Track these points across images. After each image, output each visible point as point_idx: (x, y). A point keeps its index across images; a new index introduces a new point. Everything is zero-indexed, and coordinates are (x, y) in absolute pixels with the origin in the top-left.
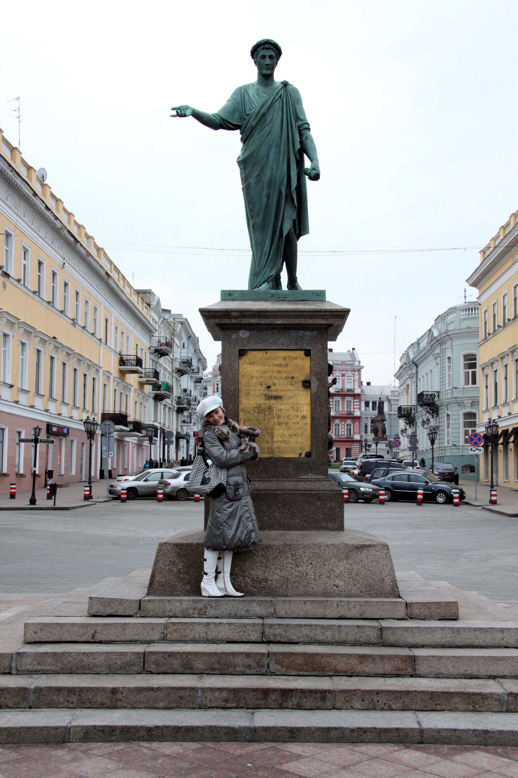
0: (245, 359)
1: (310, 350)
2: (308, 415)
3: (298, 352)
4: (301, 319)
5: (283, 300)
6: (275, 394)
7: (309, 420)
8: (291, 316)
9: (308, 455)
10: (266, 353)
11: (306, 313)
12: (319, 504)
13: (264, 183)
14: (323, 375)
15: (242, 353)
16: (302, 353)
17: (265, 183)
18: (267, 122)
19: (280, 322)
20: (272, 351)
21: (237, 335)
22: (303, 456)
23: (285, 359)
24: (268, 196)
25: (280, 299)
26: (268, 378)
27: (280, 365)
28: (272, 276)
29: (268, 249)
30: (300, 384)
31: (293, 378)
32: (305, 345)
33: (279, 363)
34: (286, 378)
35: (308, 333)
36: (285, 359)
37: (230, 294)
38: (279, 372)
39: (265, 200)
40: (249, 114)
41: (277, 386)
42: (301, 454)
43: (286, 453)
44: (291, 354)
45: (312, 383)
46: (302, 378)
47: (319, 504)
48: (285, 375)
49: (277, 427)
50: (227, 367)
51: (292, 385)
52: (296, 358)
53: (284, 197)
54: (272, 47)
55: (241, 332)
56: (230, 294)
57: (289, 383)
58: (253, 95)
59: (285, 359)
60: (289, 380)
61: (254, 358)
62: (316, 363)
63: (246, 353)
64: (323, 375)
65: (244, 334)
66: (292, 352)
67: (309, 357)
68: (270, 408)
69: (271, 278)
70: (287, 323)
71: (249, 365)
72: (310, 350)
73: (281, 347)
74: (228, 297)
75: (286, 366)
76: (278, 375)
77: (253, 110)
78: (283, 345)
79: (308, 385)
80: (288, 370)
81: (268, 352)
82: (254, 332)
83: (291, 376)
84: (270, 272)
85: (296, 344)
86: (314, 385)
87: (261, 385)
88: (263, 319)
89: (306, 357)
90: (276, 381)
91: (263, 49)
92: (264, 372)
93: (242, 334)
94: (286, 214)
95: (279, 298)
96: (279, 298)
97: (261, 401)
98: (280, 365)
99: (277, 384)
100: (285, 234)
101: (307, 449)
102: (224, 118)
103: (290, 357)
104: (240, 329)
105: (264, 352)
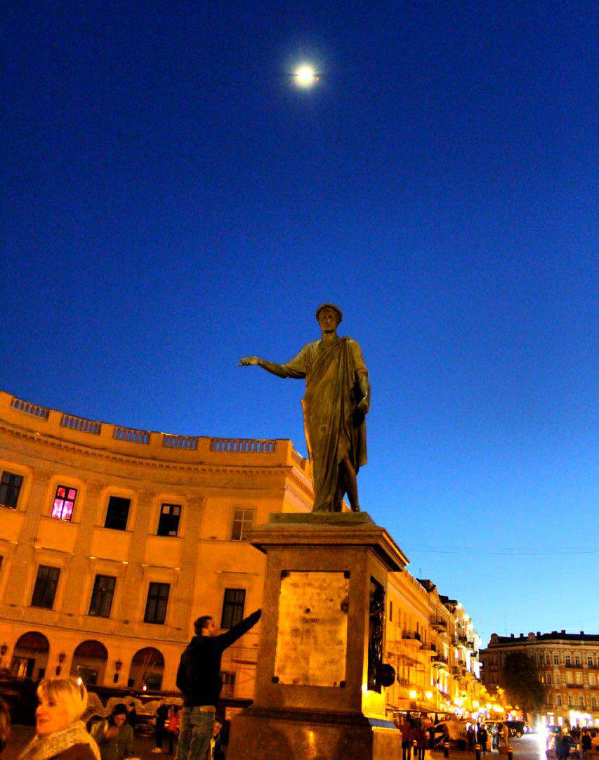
0: (288, 580)
1: (349, 572)
2: (345, 641)
3: (339, 574)
6: (314, 617)
7: (345, 646)
9: (343, 684)
12: (346, 742)
15: (285, 574)
16: (342, 574)
22: (338, 684)
24: (324, 429)
42: (335, 683)
43: (320, 681)
47: (346, 742)
49: (313, 653)
59: (324, 580)
67: (348, 580)
68: (308, 631)
72: (349, 572)
73: (321, 568)
79: (345, 608)
86: (352, 609)
87: (301, 607)
94: (340, 446)
97: (299, 625)
100: (339, 461)
101: (343, 678)
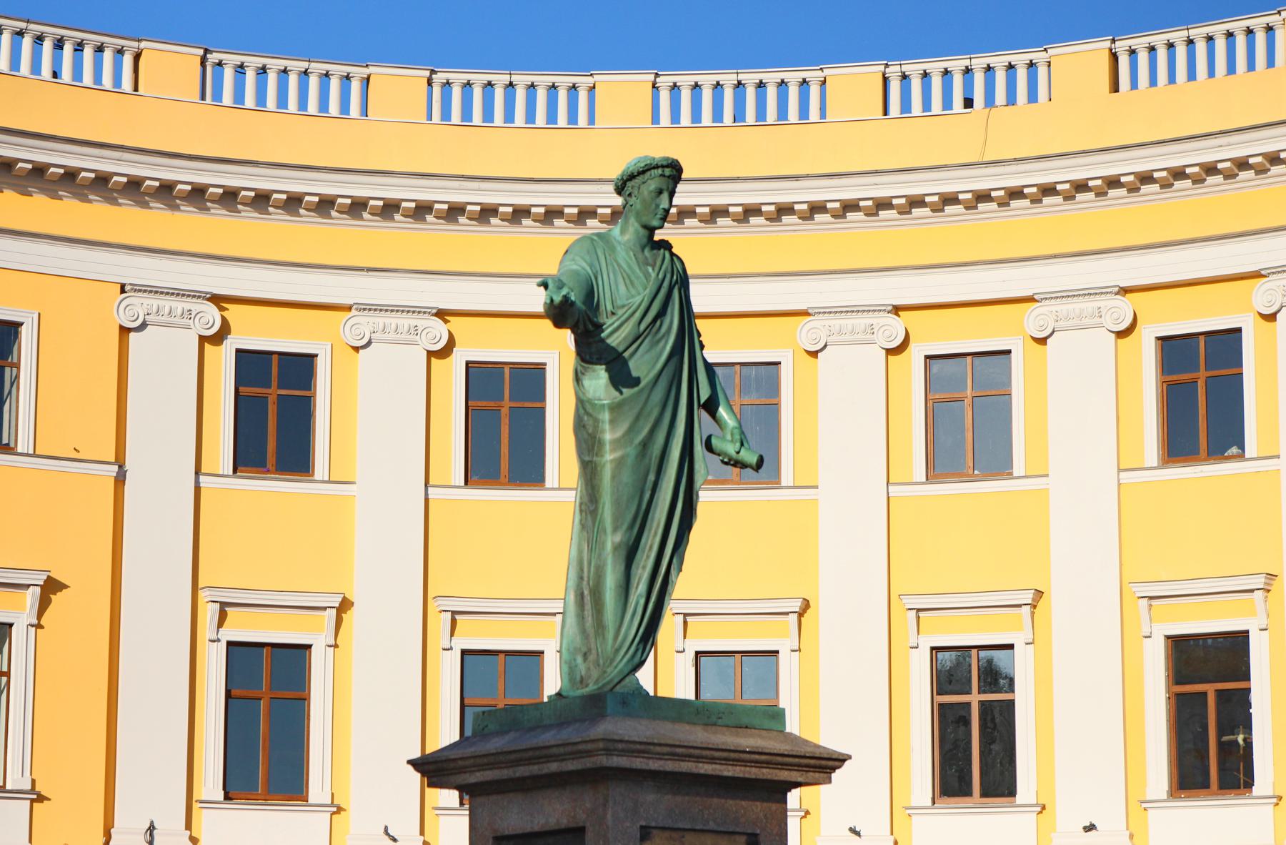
18: (663, 330)
29: (642, 601)
40: (623, 306)
73: (712, 826)
77: (638, 299)
91: (663, 175)
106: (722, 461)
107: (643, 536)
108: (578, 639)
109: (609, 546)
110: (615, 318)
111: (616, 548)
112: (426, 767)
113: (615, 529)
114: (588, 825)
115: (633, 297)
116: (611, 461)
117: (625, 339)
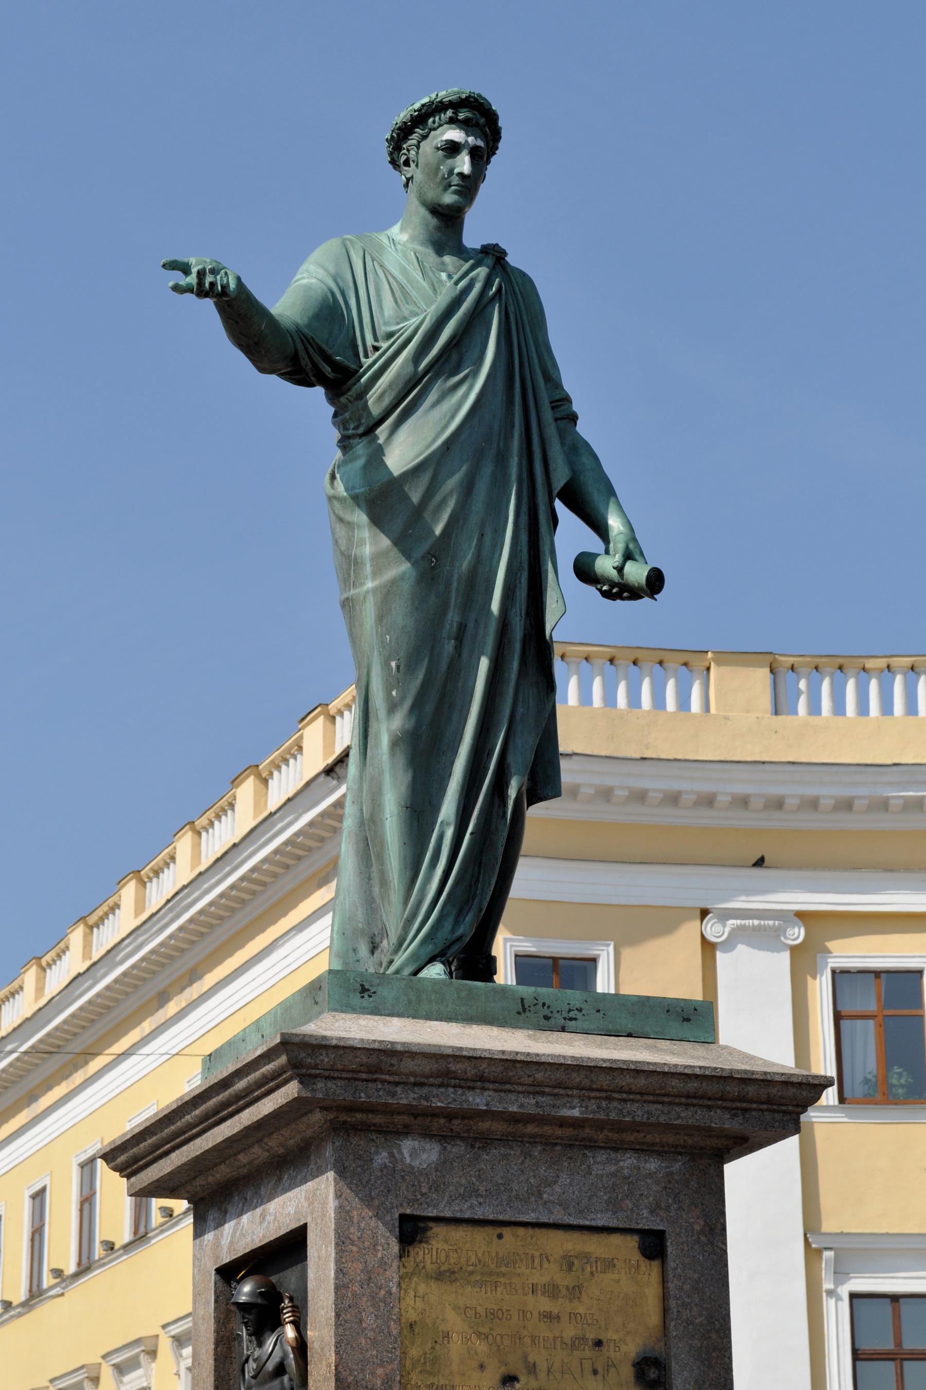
3: (616, 1239)
4: (653, 1107)
5: (563, 1030)
8: (621, 1091)
10: (500, 1236)
11: (675, 1082)
13: (448, 586)
14: (714, 1336)
15: (411, 1231)
16: (632, 1242)
17: (455, 585)
19: (576, 1113)
20: (521, 1231)
21: (392, 1155)
23: (570, 1266)
25: (552, 1020)
26: (507, 1342)
27: (552, 1291)
28: (460, 938)
29: (449, 833)
30: (627, 1372)
31: (599, 1343)
32: (645, 1213)
33: (545, 1279)
34: (576, 1343)
35: (653, 1164)
36: (568, 1263)
37: (364, 990)
38: (549, 1317)
39: (449, 647)
40: (390, 335)
41: (542, 1375)
44: (594, 1245)
45: (674, 1366)
46: (632, 1348)
48: (570, 1332)
50: (357, 1288)
51: (595, 1372)
52: (609, 1265)
53: (518, 646)
54: (482, 121)
55: (407, 1145)
56: (364, 990)
57: (587, 1365)
58: (404, 271)
59: (568, 1263)
60: (588, 1353)
61: (453, 1256)
62: (687, 1287)
63: (426, 1230)
64: (714, 1336)
65: (419, 1154)
66: (595, 1238)
67: (656, 1264)
69: (456, 948)
70: (602, 1116)
71: (433, 1285)
73: (558, 1216)
74: (356, 1000)
75: (575, 1292)
76: (544, 1330)
77: (414, 321)
78: (564, 1205)
79: (653, 1374)
80: (581, 1310)
81: (507, 1232)
82: (457, 1149)
83: (591, 1336)
84: (456, 923)
85: (614, 1206)
87: (482, 1367)
88: (513, 1097)
89: (644, 1263)
90: (538, 1357)
91: (452, 121)
92: (492, 1315)
93: (414, 1153)
94: (520, 710)
95: (546, 1018)
96: (546, 1018)
98: (552, 1291)
99: (542, 1366)
102: (306, 331)
103: (586, 1257)
104: (405, 1132)
105: (492, 1232)
106: (605, 594)
107: (481, 741)
108: (360, 915)
109: (385, 741)
110: (377, 354)
111: (395, 744)
112: (122, 1158)
113: (392, 708)
114: (309, 1220)
115: (405, 319)
116: (375, 590)
117: (391, 385)
